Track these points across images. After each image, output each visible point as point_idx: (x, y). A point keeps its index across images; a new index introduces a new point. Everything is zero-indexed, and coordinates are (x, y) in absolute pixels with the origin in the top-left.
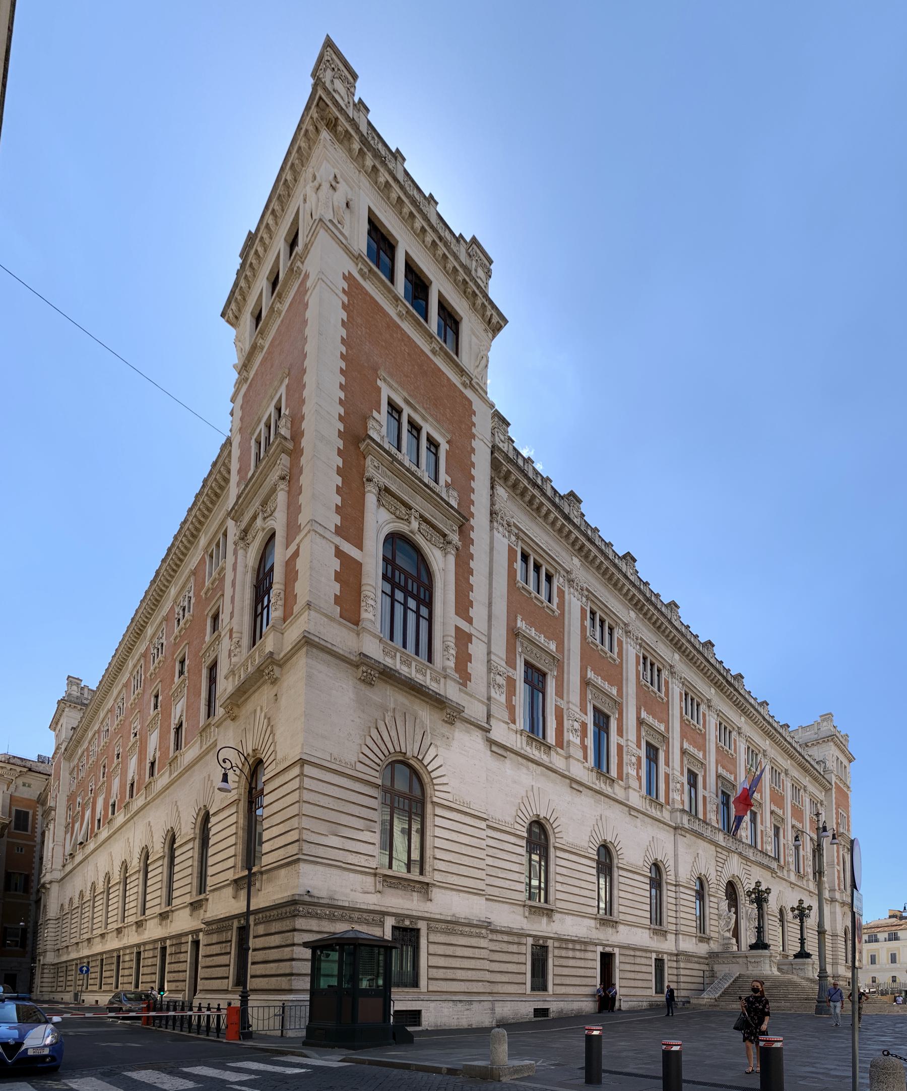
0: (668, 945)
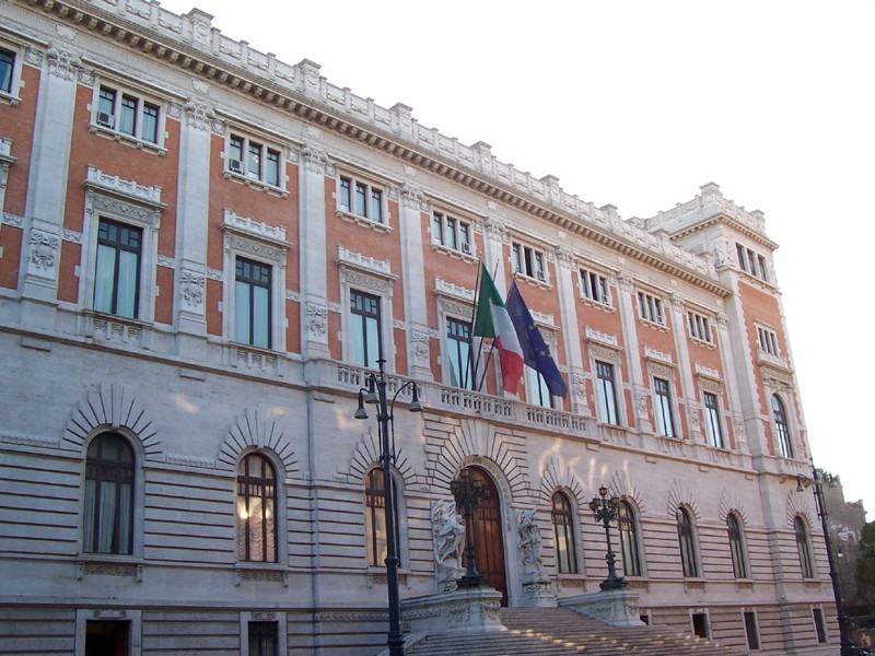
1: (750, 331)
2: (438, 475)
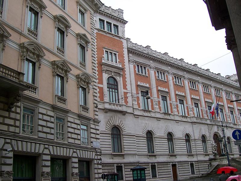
0: (195, 159)
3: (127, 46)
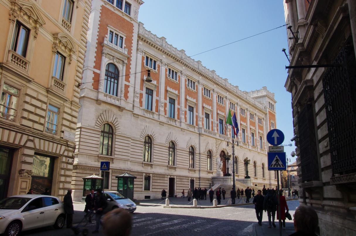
0: (196, 175)
1: (270, 122)
2: (218, 152)
3: (138, 32)
